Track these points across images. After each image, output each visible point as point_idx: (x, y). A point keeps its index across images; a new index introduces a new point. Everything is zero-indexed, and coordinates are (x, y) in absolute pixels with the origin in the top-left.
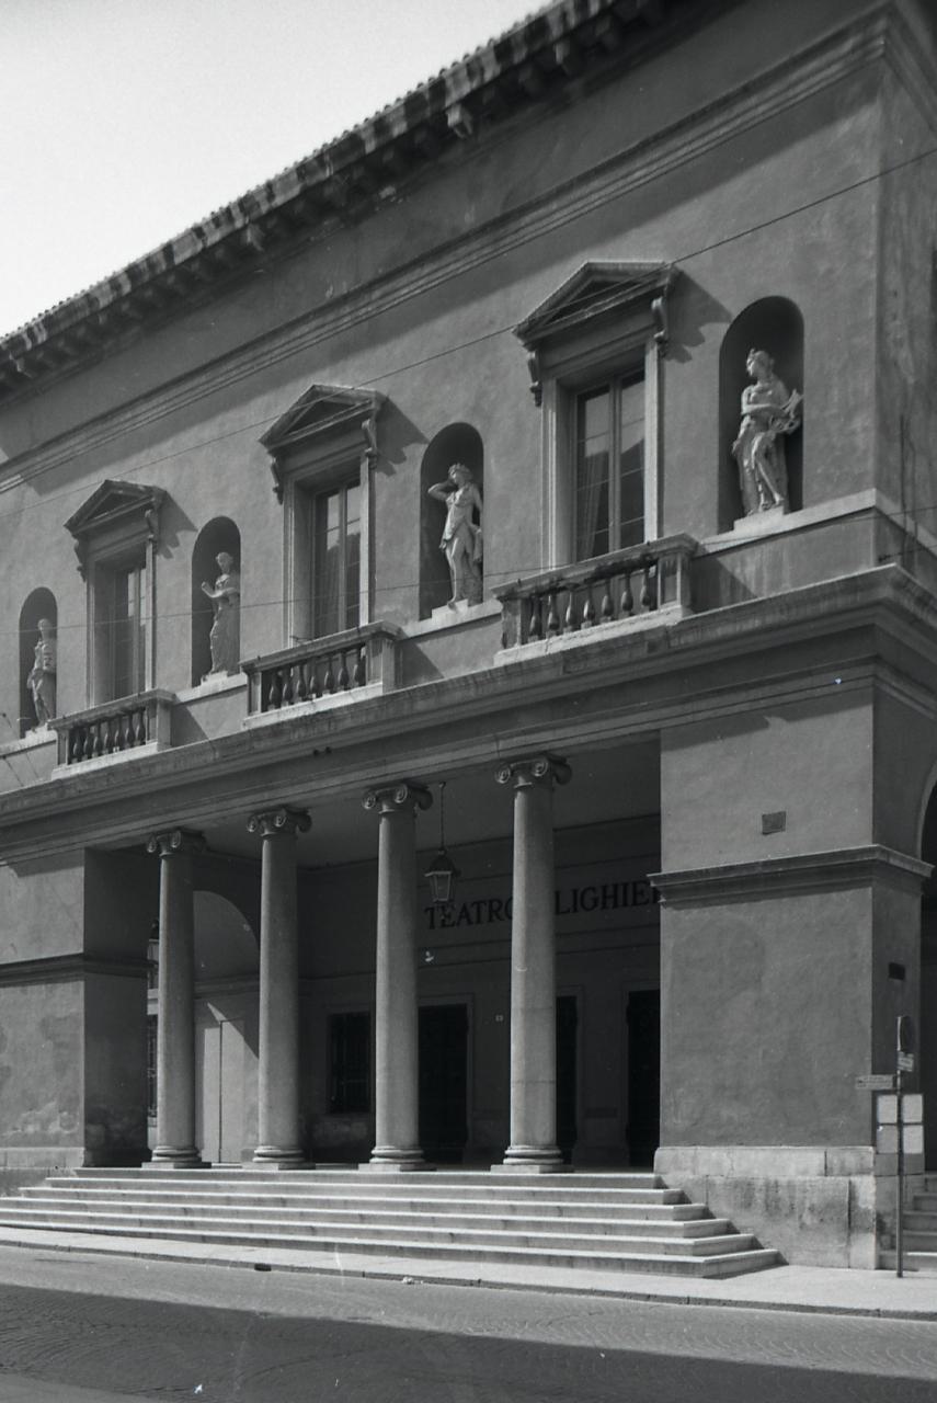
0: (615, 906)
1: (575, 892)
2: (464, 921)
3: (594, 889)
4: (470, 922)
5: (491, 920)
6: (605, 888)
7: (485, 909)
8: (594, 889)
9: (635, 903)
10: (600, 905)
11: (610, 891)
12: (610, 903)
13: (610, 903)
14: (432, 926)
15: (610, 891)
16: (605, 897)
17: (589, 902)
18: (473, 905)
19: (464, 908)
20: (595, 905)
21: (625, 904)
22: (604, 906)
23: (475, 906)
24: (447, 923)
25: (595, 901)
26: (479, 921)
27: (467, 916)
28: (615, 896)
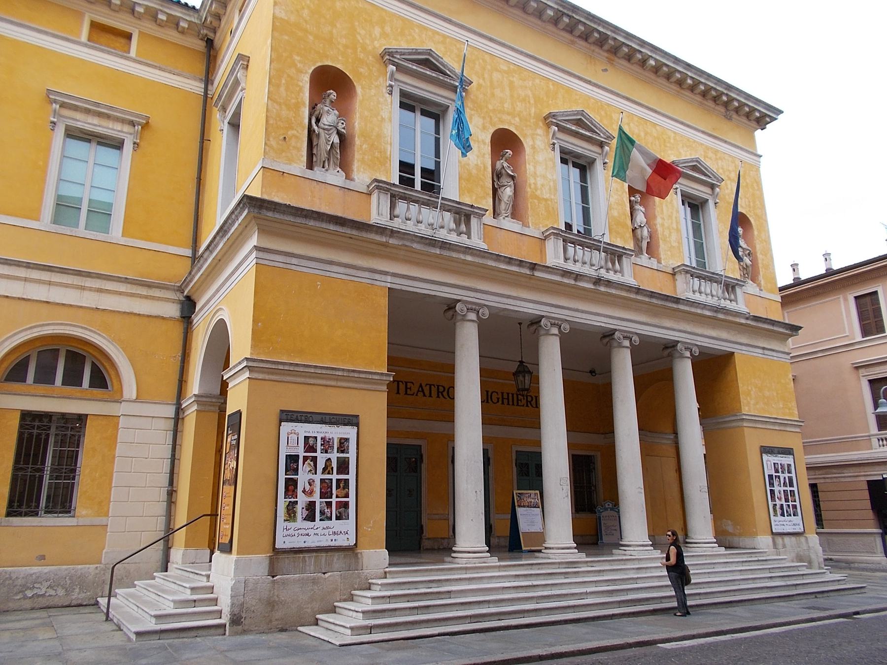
0: (508, 404)
1: (487, 392)
2: (420, 394)
3: (497, 393)
4: (424, 395)
5: (438, 397)
6: (502, 393)
7: (434, 390)
8: (497, 393)
9: (518, 405)
10: (500, 402)
11: (505, 396)
12: (505, 401)
13: (505, 401)
14: (398, 393)
15: (505, 396)
16: (503, 398)
17: (495, 396)
18: (427, 384)
19: (421, 386)
20: (498, 401)
21: (513, 404)
22: (503, 403)
23: (428, 387)
24: (408, 393)
25: (498, 399)
26: (430, 396)
27: (423, 391)
28: (508, 399)
